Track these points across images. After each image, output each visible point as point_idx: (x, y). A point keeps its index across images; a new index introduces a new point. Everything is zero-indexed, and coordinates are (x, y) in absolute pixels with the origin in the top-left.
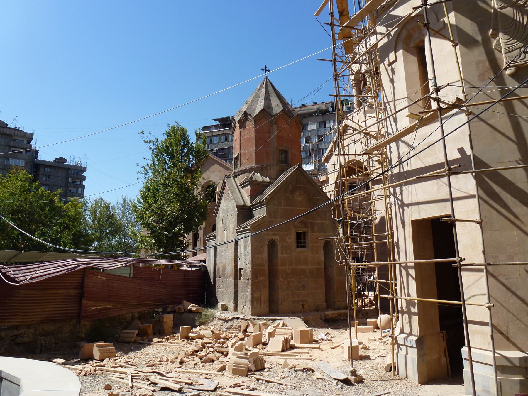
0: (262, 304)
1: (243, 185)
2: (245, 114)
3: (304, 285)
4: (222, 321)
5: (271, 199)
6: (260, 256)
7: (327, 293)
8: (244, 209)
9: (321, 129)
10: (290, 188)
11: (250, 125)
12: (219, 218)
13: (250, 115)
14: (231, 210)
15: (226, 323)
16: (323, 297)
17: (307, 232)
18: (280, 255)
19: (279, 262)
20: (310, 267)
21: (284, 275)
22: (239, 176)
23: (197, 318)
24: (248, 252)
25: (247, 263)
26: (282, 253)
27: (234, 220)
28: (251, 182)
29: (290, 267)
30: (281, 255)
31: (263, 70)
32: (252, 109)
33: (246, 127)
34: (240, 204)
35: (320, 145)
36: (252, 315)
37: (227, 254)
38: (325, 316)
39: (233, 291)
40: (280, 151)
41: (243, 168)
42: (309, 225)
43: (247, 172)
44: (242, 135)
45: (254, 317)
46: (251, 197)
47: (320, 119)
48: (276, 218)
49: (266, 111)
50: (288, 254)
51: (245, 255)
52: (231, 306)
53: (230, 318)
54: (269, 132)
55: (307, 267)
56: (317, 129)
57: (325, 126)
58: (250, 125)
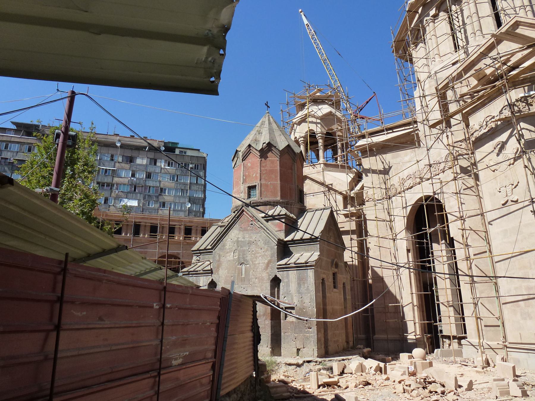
1: (269, 218)
4: (295, 366)
9: (151, 166)
14: (261, 243)
15: (298, 368)
24: (308, 289)
27: (269, 253)
35: (147, 182)
36: (318, 357)
41: (265, 199)
43: (270, 205)
46: (285, 233)
47: (152, 155)
51: (299, 292)
56: (146, 165)
57: (155, 164)
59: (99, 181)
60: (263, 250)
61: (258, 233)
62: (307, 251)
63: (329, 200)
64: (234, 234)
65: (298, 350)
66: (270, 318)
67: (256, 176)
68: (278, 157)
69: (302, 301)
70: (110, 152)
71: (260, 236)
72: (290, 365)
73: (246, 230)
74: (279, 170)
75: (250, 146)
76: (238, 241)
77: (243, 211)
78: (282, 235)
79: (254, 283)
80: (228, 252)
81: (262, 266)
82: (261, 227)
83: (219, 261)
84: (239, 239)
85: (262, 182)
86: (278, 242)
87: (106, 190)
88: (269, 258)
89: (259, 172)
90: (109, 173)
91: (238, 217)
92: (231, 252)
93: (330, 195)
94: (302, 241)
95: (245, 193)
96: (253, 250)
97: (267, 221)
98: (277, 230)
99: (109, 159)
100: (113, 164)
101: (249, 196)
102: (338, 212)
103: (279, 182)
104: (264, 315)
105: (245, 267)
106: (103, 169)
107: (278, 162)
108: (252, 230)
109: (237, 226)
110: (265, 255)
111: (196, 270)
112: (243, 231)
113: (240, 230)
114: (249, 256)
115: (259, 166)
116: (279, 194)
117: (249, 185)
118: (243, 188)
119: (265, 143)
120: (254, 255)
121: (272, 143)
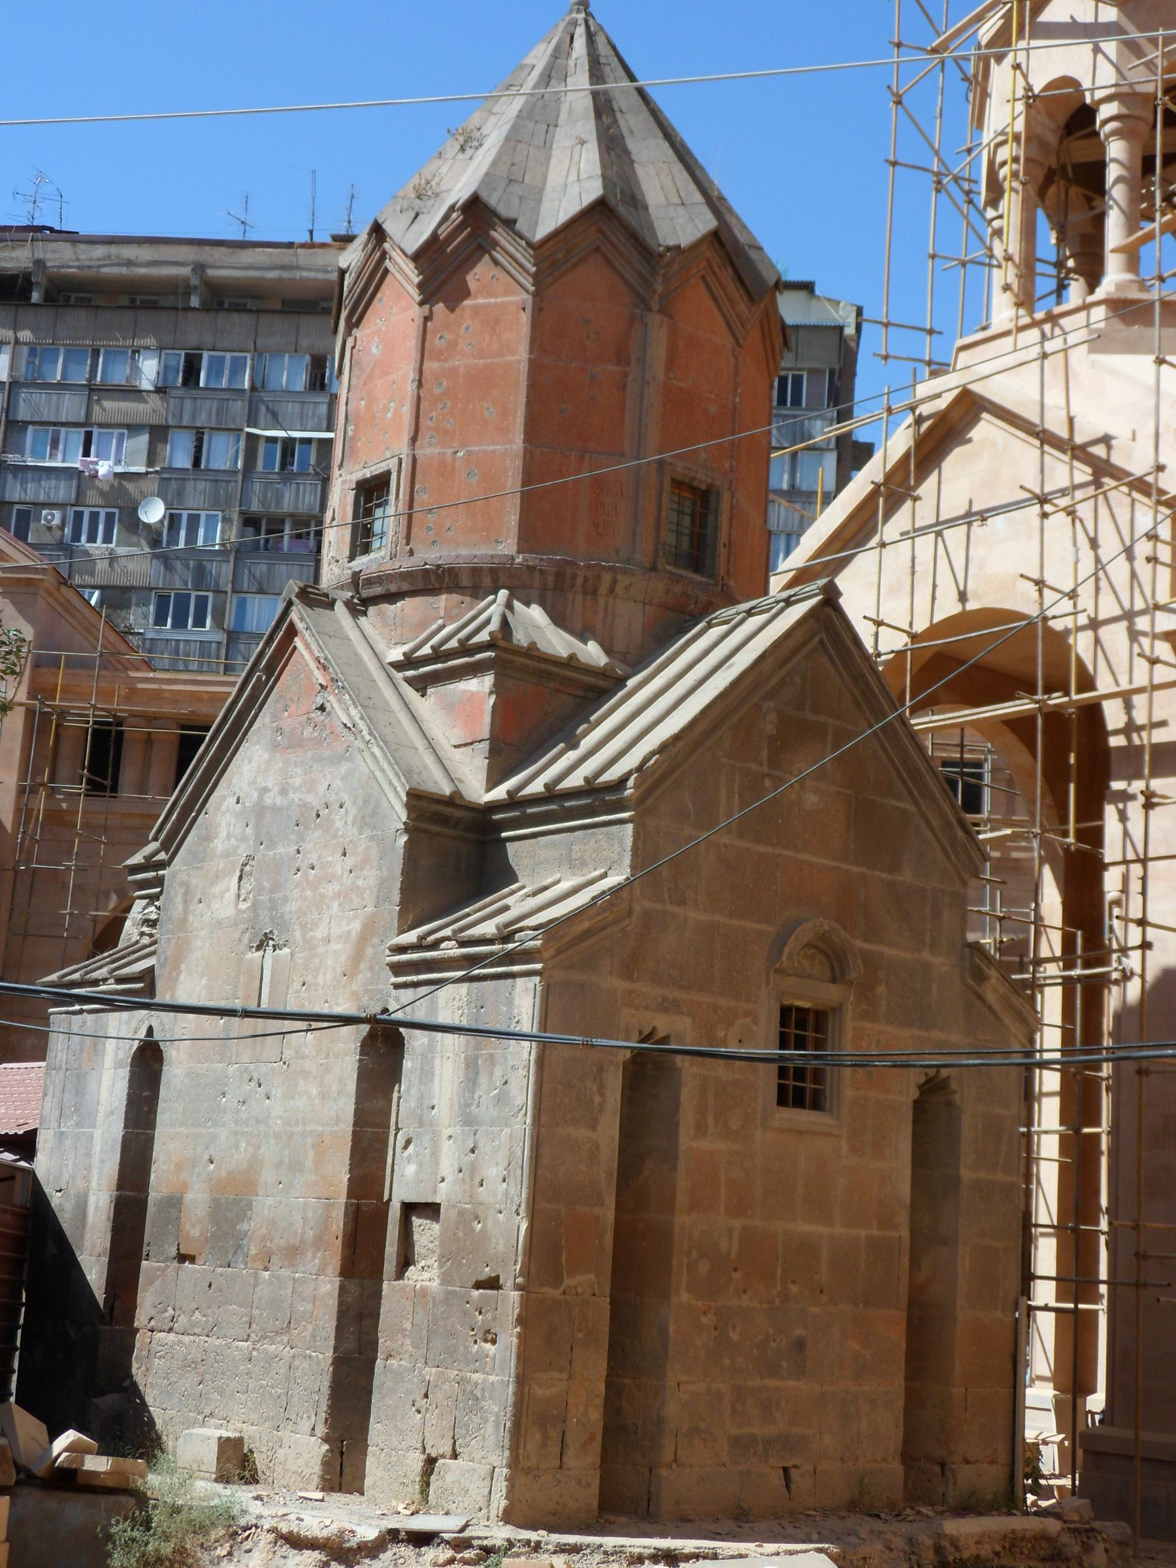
0: (570, 1452)
1: (426, 671)
2: (476, 211)
3: (800, 1345)
5: (664, 777)
6: (580, 1133)
7: (914, 1400)
8: (445, 821)
10: (769, 726)
11: (501, 295)
12: (198, 859)
13: (510, 223)
14: (343, 823)
16: (883, 1426)
17: (837, 1010)
18: (686, 1139)
19: (682, 1183)
20: (839, 1230)
21: (704, 1268)
22: (390, 609)
23: (120, 1529)
24: (502, 1099)
25: (493, 1172)
26: (701, 1129)
27: (369, 879)
28: (508, 659)
29: (737, 1224)
30: (696, 1142)
32: (517, 189)
33: (466, 293)
34: (431, 788)
36: (508, 1517)
37: (276, 1107)
38: (938, 1549)
39: (326, 1357)
40: (677, 484)
41: (429, 556)
42: (856, 970)
44: (436, 342)
45: (533, 1536)
46: (494, 752)
48: (682, 902)
49: (611, 219)
50: (729, 1137)
51: (469, 1121)
52: (302, 1448)
53: (368, 1533)
54: (621, 357)
55: (825, 1230)
58: (501, 295)
59: (255, 507)
60: (350, 861)
61: (337, 760)
62: (574, 864)
63: (1094, 544)
65: (431, 1462)
66: (335, 1264)
67: (398, 415)
69: (473, 1168)
70: (305, 342)
72: (296, 1542)
73: (296, 743)
74: (524, 367)
76: (260, 810)
77: (292, 632)
79: (299, 1055)
80: (218, 876)
81: (336, 955)
83: (184, 920)
84: (268, 800)
85: (428, 450)
86: (409, 806)
87: (291, 557)
88: (370, 909)
89: (410, 388)
90: (304, 463)
91: (270, 669)
93: (1103, 510)
94: (559, 806)
96: (313, 858)
97: (421, 685)
98: (452, 740)
99: (301, 382)
100: (323, 409)
102: (1142, 623)
103: (518, 443)
104: (318, 1242)
105: (276, 960)
106: (273, 440)
107: (525, 318)
108: (319, 742)
109: (264, 720)
110: (355, 889)
111: (95, 975)
113: (275, 747)
114: (296, 893)
115: (414, 355)
116: (513, 519)
120: (315, 888)
121: (493, 199)
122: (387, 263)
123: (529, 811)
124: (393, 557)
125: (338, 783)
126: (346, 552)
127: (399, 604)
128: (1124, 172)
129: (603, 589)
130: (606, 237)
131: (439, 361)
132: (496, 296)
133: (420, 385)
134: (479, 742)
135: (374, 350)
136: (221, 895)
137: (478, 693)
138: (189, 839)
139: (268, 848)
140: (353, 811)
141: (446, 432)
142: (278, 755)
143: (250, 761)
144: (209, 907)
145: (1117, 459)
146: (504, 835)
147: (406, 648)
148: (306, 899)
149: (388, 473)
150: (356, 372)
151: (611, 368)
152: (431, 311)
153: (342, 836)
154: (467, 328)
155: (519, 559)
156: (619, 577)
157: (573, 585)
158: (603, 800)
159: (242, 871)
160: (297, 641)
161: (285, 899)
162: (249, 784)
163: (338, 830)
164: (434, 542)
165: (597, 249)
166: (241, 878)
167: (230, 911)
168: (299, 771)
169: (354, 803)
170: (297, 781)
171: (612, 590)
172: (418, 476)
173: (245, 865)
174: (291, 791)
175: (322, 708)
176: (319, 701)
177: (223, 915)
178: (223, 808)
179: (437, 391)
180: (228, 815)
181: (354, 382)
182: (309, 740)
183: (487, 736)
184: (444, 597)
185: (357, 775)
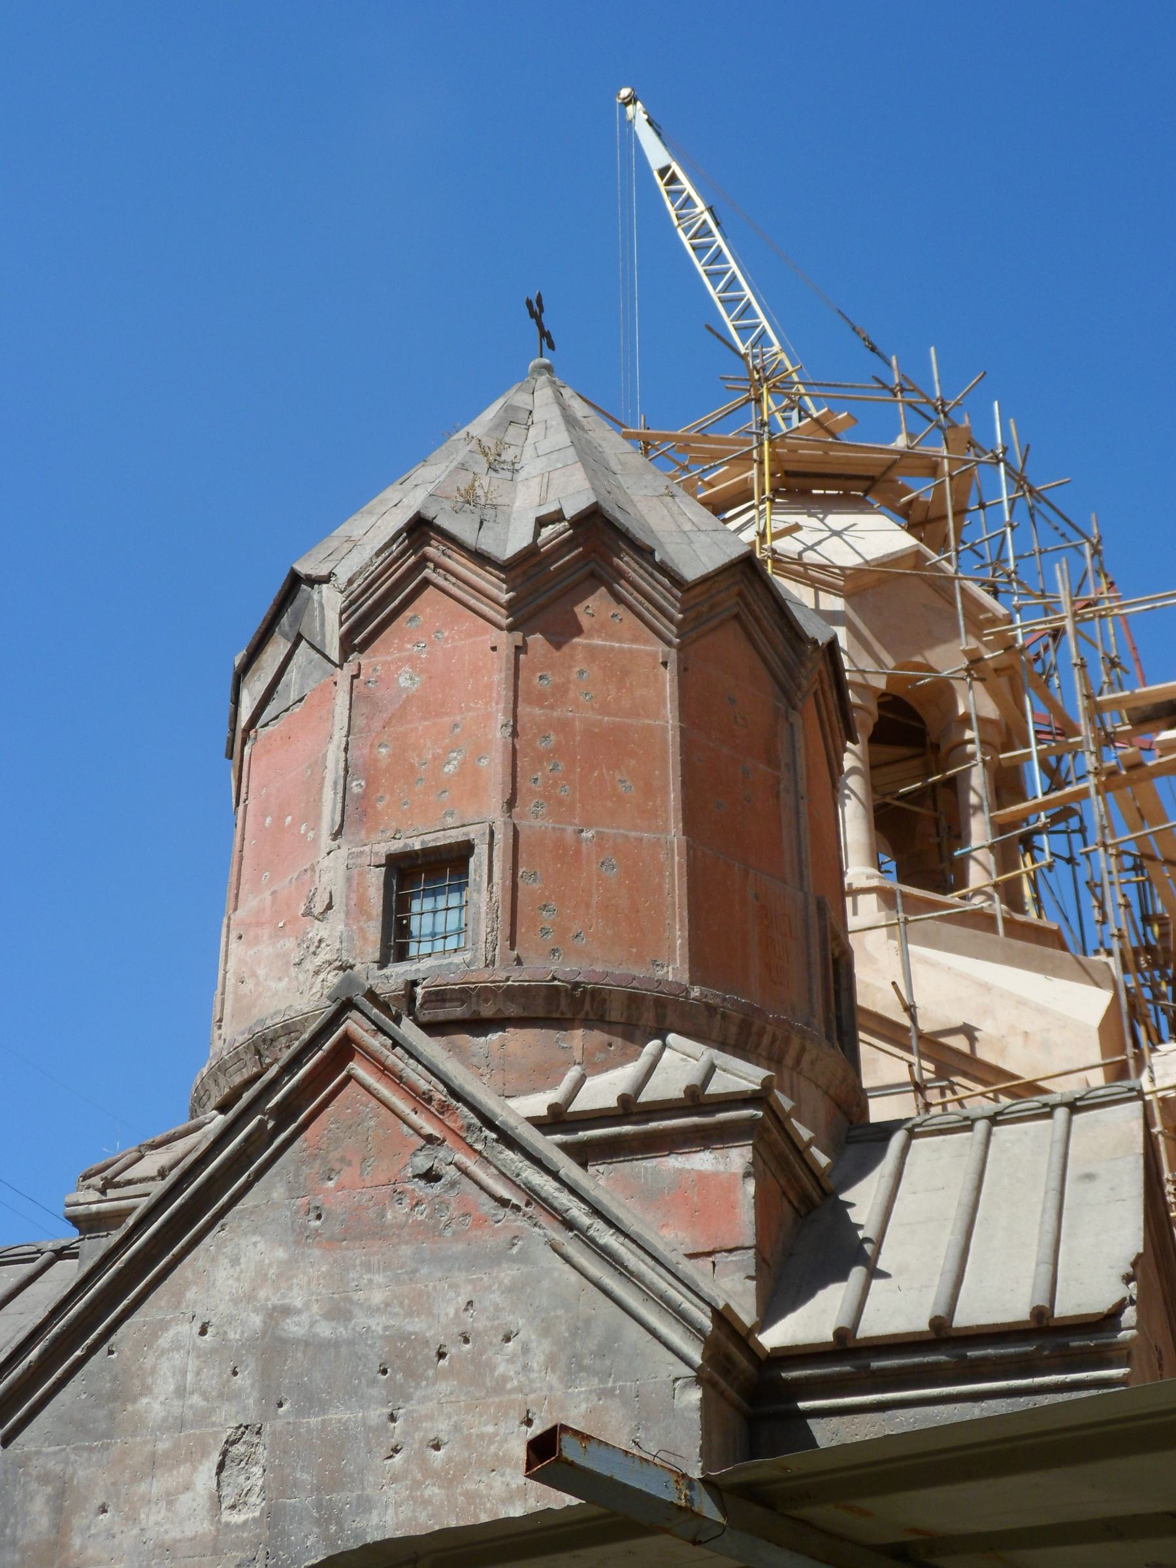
31: (529, 304)
33: (578, 631)
44: (533, 682)
61: (497, 1258)
64: (236, 1272)
68: (670, 631)
71: (511, 1290)
73: (363, 1230)
74: (672, 737)
75: (419, 529)
76: (271, 1348)
77: (347, 1049)
78: (736, 1289)
80: (154, 1463)
82: (533, 1196)
84: (293, 1328)
89: (498, 734)
91: (286, 1112)
92: (194, 1456)
95: (359, 909)
96: (441, 1428)
101: (396, 942)
103: (675, 835)
107: (668, 678)
108: (432, 1230)
109: (271, 1193)
112: (332, 1242)
113: (302, 1237)
114: (390, 1493)
116: (679, 936)
117: (397, 846)
118: (345, 872)
119: (557, 516)
122: (428, 572)
123: (875, 1364)
124: (489, 963)
125: (496, 1297)
126: (373, 951)
127: (494, 1037)
128: (858, 764)
129: (789, 1061)
130: (747, 604)
131: (542, 707)
132: (620, 641)
133: (514, 734)
134: (730, 1251)
135: (403, 682)
136: (170, 1499)
137: (715, 1174)
138: (63, 1396)
139: (301, 1412)
140: (541, 1350)
141: (560, 802)
142: (317, 1252)
143: (235, 1261)
144: (132, 1519)
145: (984, 1053)
146: (802, 1405)
147: (553, 1096)
148: (426, 1502)
149: (467, 848)
150: (362, 708)
151: (762, 767)
152: (524, 641)
153: (520, 1389)
154: (581, 672)
155: (696, 992)
156: (808, 1046)
157: (758, 1045)
158: (1067, 1346)
159: (225, 1453)
160: (356, 1067)
161: (365, 1505)
162: (236, 1302)
163: (505, 1379)
164: (554, 951)
165: (736, 617)
166: (221, 1467)
167: (201, 1526)
168: (379, 1278)
169: (546, 1331)
170: (378, 1297)
171: (798, 1061)
172: (523, 856)
173: (231, 1443)
174: (356, 1311)
175: (430, 1176)
176: (422, 1162)
177: (175, 1533)
178: (165, 1340)
179: (542, 746)
180: (177, 1357)
181: (359, 722)
182: (401, 1227)
183: (749, 1238)
184: (579, 1033)
185: (546, 1284)
